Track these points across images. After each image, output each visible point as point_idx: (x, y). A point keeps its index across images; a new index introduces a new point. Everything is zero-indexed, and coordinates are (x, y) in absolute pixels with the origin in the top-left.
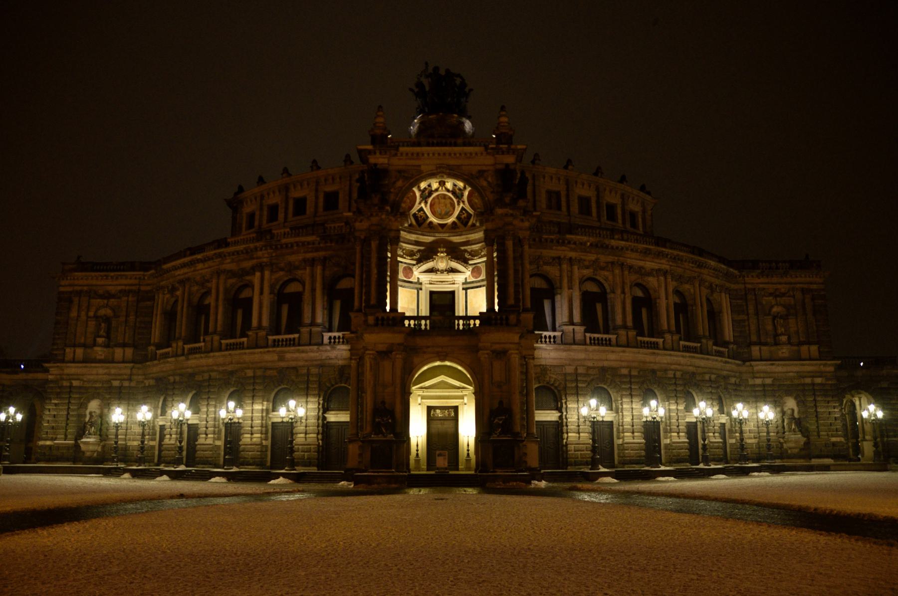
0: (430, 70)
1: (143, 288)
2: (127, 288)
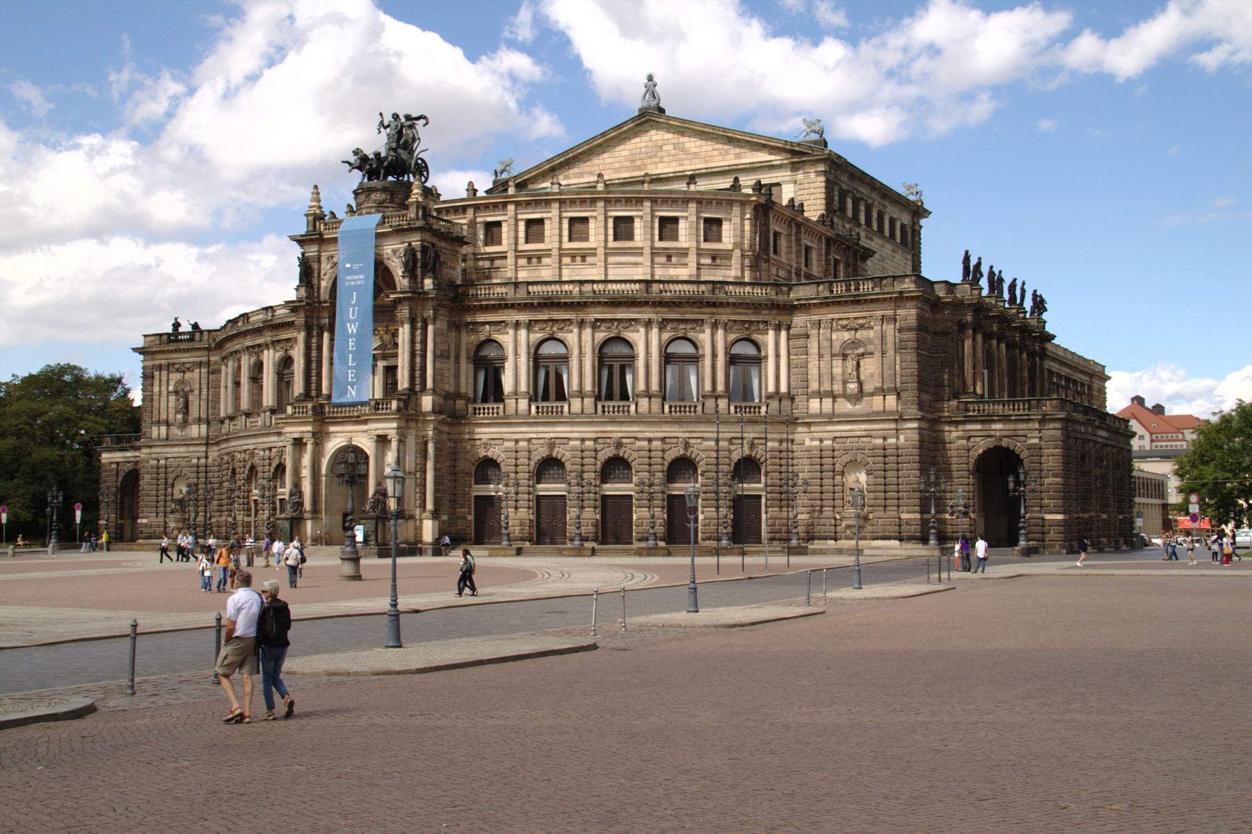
0: (388, 119)
1: (212, 359)
2: (199, 359)
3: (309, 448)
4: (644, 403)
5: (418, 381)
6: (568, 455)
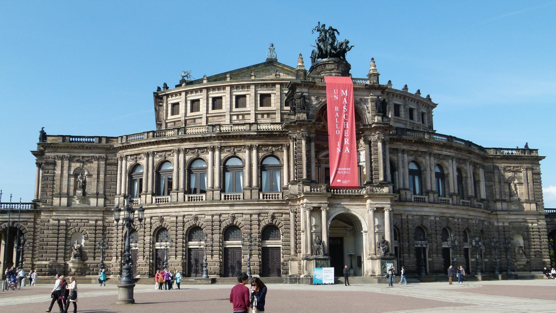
2: (97, 155)
3: (324, 214)
4: (455, 197)
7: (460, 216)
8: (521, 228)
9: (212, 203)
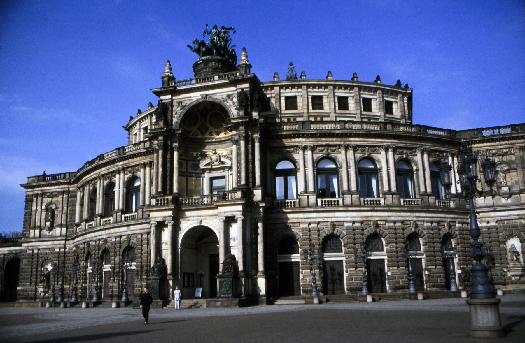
1: (71, 189)
2: (62, 190)
4: (389, 197)
5: (251, 180)
6: (344, 232)
7: (399, 219)
8: (515, 226)
9: (118, 224)
